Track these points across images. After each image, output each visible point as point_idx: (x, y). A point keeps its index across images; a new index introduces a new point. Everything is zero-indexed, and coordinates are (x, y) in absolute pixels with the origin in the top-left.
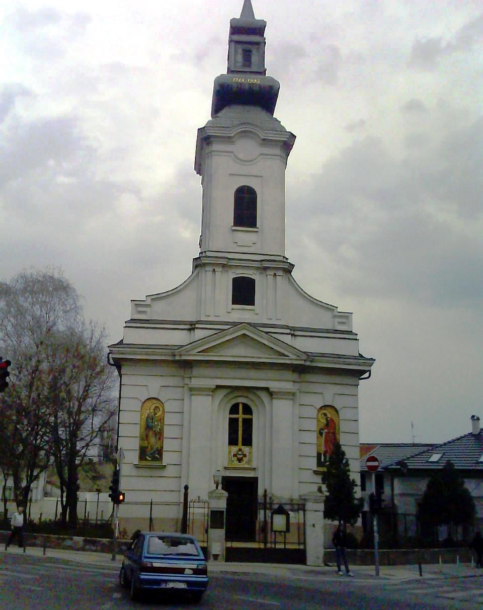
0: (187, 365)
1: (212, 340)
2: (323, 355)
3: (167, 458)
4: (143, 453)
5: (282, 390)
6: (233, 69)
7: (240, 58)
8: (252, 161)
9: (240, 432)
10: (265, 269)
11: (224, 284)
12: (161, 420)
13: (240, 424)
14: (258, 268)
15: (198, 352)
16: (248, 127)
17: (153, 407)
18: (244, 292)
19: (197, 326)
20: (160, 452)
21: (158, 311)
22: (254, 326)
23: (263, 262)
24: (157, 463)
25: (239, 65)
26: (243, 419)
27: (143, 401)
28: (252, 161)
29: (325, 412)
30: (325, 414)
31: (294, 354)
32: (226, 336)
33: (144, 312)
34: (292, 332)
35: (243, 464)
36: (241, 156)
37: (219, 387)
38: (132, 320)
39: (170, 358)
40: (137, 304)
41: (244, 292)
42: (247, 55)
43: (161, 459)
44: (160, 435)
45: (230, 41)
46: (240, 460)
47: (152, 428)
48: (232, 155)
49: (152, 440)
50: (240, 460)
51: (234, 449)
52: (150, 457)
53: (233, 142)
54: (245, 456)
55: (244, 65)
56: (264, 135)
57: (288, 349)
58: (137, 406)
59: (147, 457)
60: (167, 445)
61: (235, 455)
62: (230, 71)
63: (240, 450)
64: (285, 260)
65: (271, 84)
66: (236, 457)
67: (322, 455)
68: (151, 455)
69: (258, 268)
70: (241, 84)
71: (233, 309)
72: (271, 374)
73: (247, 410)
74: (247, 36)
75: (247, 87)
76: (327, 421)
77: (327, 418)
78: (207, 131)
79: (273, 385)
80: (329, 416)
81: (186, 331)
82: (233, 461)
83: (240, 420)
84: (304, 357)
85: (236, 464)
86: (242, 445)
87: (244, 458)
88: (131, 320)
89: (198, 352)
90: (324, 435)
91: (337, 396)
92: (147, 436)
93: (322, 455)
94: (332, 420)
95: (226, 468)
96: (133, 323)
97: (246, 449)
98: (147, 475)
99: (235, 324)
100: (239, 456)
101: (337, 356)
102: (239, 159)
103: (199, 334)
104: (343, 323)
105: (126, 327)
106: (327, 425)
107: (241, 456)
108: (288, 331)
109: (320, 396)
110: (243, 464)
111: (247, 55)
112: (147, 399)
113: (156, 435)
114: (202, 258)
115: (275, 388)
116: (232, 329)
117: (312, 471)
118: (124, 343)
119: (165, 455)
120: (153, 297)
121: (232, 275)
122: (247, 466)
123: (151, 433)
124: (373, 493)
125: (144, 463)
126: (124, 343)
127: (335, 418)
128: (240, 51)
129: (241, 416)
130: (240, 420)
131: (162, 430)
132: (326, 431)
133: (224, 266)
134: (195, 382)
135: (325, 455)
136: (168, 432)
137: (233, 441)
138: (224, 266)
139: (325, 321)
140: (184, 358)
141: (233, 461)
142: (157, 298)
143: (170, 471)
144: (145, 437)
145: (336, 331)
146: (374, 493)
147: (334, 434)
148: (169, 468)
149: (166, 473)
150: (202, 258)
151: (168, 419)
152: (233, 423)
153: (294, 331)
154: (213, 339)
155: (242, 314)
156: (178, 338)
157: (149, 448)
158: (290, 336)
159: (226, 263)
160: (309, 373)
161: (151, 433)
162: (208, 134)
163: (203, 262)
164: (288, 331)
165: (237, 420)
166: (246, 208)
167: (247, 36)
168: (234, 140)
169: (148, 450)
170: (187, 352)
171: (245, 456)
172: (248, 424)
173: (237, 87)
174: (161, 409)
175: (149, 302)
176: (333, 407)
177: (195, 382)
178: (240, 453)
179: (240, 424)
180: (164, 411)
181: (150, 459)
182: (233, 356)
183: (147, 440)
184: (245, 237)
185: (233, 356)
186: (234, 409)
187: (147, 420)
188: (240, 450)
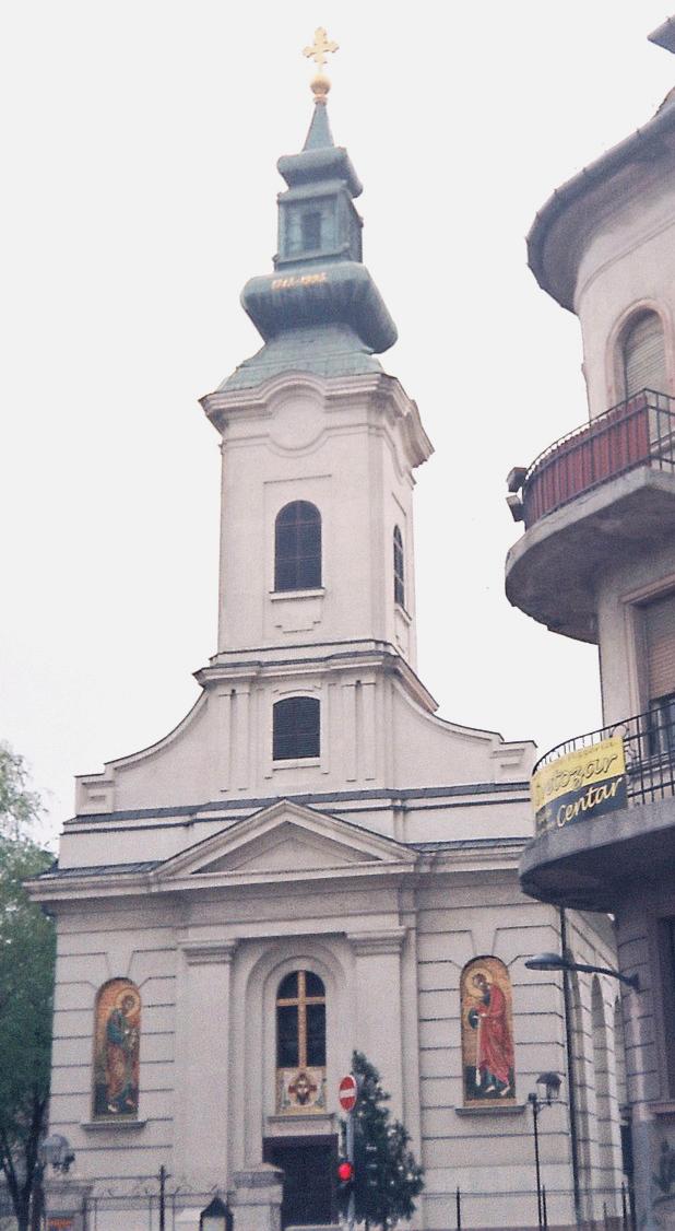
0: (180, 902)
1: (221, 842)
2: (463, 845)
3: (146, 1107)
4: (101, 1098)
5: (372, 935)
6: (282, 260)
7: (297, 234)
8: (312, 444)
9: (302, 1037)
10: (339, 673)
11: (257, 717)
12: (135, 1024)
13: (302, 1018)
14: (323, 676)
15: (193, 873)
16: (288, 378)
17: (121, 997)
18: (297, 731)
19: (200, 815)
20: (134, 1092)
21: (135, 792)
22: (304, 801)
23: (329, 662)
24: (128, 1120)
25: (296, 247)
26: (309, 1008)
27: (99, 985)
28: (312, 444)
29: (482, 971)
30: (481, 977)
31: (391, 853)
32: (248, 831)
33: (102, 798)
34: (399, 803)
35: (310, 1108)
36: (287, 441)
37: (243, 943)
38: (81, 818)
39: (143, 891)
40: (87, 783)
41: (297, 731)
42: (312, 225)
43: (132, 1110)
44: (132, 1057)
45: (285, 204)
46: (303, 1099)
47: (117, 1042)
48: (266, 440)
49: (120, 1069)
50: (303, 1099)
51: (290, 1075)
52: (113, 1106)
53: (270, 414)
54: (314, 1088)
55: (307, 246)
56: (327, 388)
57: (380, 844)
58: (87, 998)
59: (110, 1107)
60: (147, 1077)
61: (292, 1089)
62: (280, 265)
63: (302, 1076)
64: (381, 648)
65: (349, 277)
66: (294, 1095)
67: (478, 1071)
68: (115, 1101)
69: (323, 676)
70: (289, 290)
71: (275, 770)
72: (353, 902)
73: (315, 985)
74: (320, 191)
75: (301, 294)
76: (485, 990)
77: (485, 985)
78: (212, 402)
79: (355, 927)
80: (489, 979)
81: (181, 828)
82: (287, 1103)
83: (302, 1009)
84: (411, 856)
85: (295, 1107)
86: (308, 1065)
87: (312, 1095)
88: (78, 817)
89: (193, 873)
90: (479, 1026)
91: (501, 933)
92: (110, 1062)
93: (478, 1071)
94: (496, 988)
95: (272, 1120)
96: (83, 824)
97: (314, 1074)
98: (110, 1145)
99: (265, 804)
100: (300, 1091)
101: (492, 844)
102: (281, 447)
103: (202, 831)
104: (516, 766)
105: (65, 833)
106: (486, 1001)
107: (306, 1090)
108: (388, 803)
109: (466, 936)
110: (310, 1108)
111: (312, 225)
112: (107, 983)
113: (126, 1057)
114: (204, 671)
115: (357, 933)
116: (262, 814)
117: (450, 1113)
118: (60, 867)
119: (142, 1098)
120: (117, 765)
121: (270, 698)
122: (318, 1111)
123: (117, 1054)
124: (276, 1173)
125: (105, 1121)
126: (60, 867)
127: (501, 983)
128: (297, 219)
129: (301, 1001)
130: (302, 1009)
131: (137, 1045)
132: (484, 1015)
133: (253, 681)
134: (196, 937)
135: (483, 1070)
136: (148, 1049)
137: (286, 1058)
138: (253, 681)
139: (478, 768)
140: (166, 888)
141: (287, 1103)
142: (124, 766)
143: (153, 1135)
144: (101, 1065)
145: (498, 788)
146: (279, 1170)
147: (502, 1019)
148: (153, 1127)
149: (147, 1138)
150: (204, 671)
151: (149, 1021)
152: (286, 1017)
153: (400, 802)
154: (225, 840)
155: (297, 778)
156: (161, 845)
157: (114, 1086)
158: (391, 813)
159: (254, 674)
160: (441, 888)
161: (117, 1054)
162: (215, 407)
163: (208, 678)
164: (388, 803)
165: (294, 1009)
166: (298, 550)
167: (320, 191)
168: (270, 409)
169: (111, 1091)
170: (172, 874)
171: (314, 1088)
172: (317, 1014)
173: (283, 296)
174: (137, 999)
175: (108, 777)
176: (118, 979)
177: (196, 937)
178: (302, 1083)
179: (302, 1018)
180: (140, 1005)
181: (114, 1110)
182: (273, 873)
183: (110, 1071)
184: (300, 612)
185: (273, 873)
186: (288, 987)
187: (109, 1028)
188: (302, 1076)
